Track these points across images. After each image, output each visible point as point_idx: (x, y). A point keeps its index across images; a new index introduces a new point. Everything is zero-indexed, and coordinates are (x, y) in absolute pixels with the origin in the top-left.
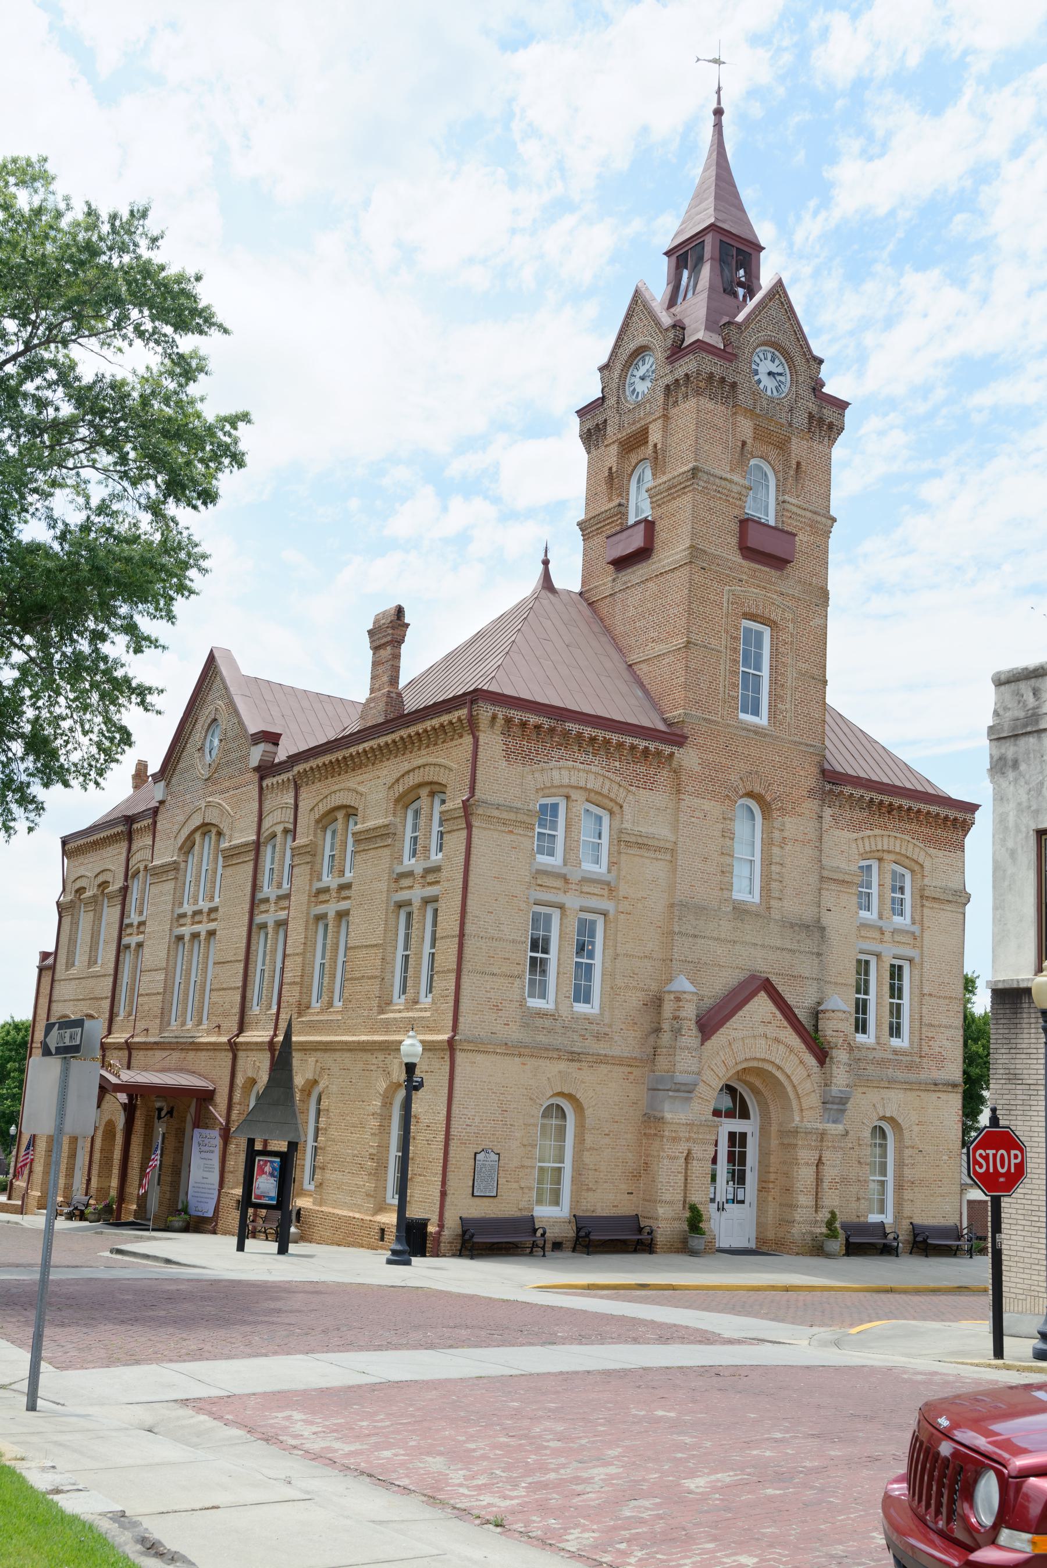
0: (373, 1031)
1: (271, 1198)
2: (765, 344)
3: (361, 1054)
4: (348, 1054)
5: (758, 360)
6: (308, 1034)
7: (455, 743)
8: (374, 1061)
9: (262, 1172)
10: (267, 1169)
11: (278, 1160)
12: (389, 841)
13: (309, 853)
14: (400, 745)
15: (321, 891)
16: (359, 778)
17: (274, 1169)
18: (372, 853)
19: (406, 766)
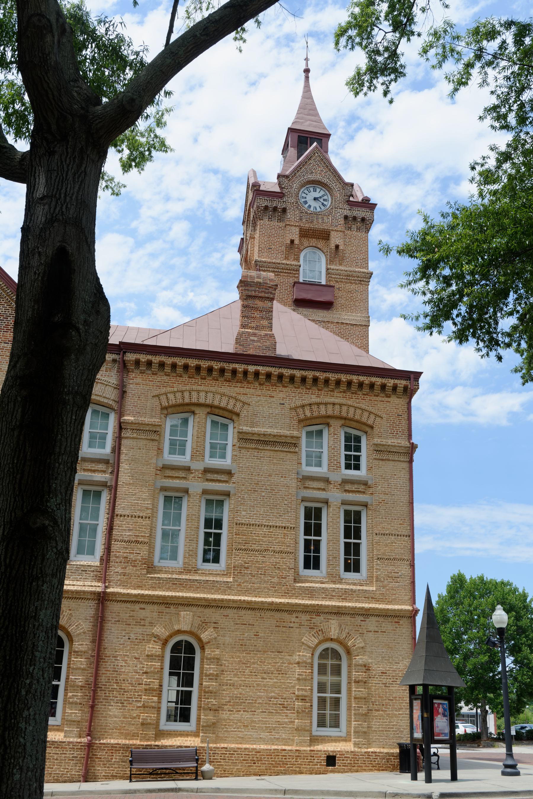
0: (286, 594)
1: (445, 734)
2: (302, 186)
3: (269, 614)
4: (249, 612)
5: (304, 195)
6: (174, 590)
7: (380, 399)
8: (293, 620)
9: (438, 713)
10: (441, 710)
11: (446, 702)
12: (297, 449)
13: (154, 432)
14: (309, 381)
15: (165, 467)
16: (236, 389)
17: (445, 710)
18: (268, 453)
19: (314, 399)
